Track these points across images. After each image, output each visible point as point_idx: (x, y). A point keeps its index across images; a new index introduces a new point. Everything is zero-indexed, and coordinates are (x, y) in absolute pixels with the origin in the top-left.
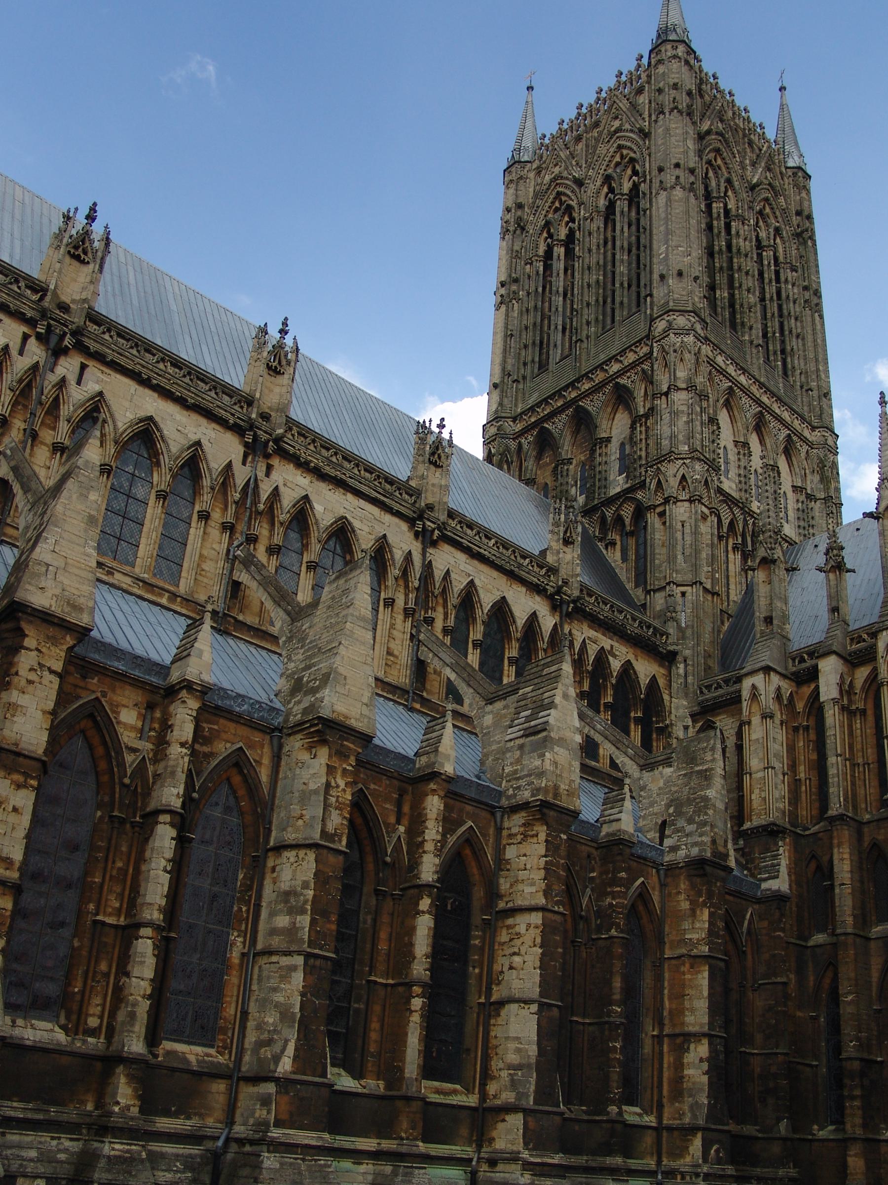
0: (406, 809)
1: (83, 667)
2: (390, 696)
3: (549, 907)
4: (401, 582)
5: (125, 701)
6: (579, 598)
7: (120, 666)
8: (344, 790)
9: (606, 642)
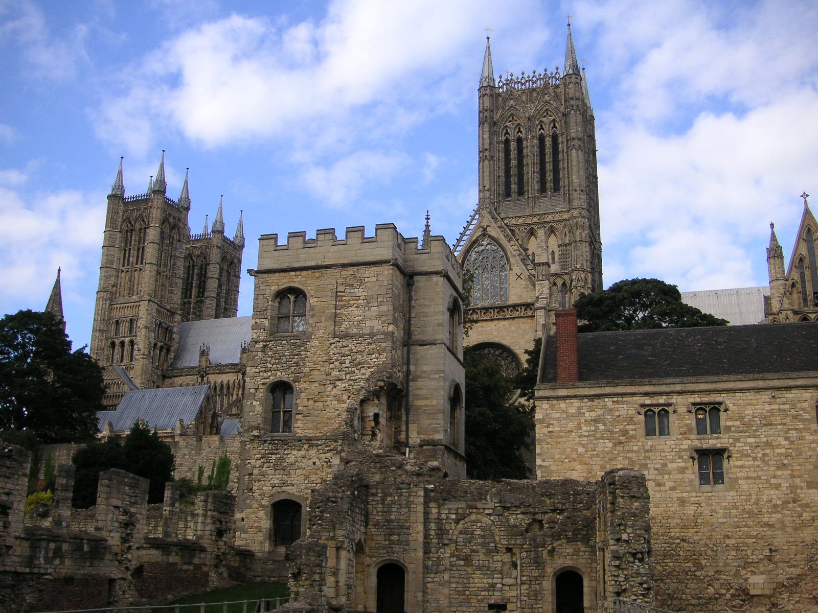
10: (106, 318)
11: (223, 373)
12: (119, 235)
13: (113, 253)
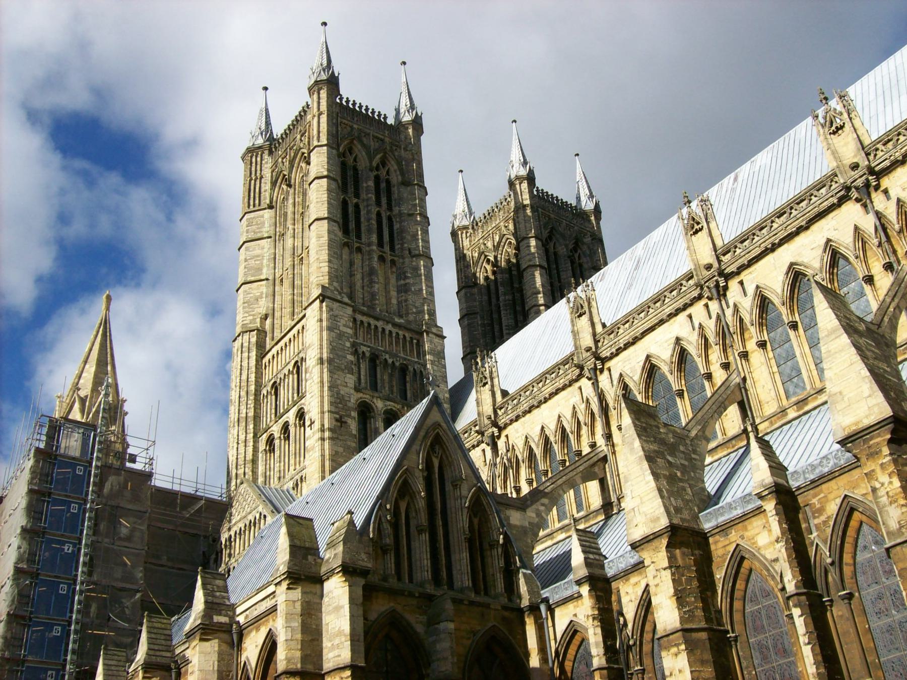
1: (723, 530)
5: (757, 531)
7: (739, 512)
8: (891, 483)
10: (252, 388)
11: (538, 407)
12: (268, 214)
13: (258, 252)
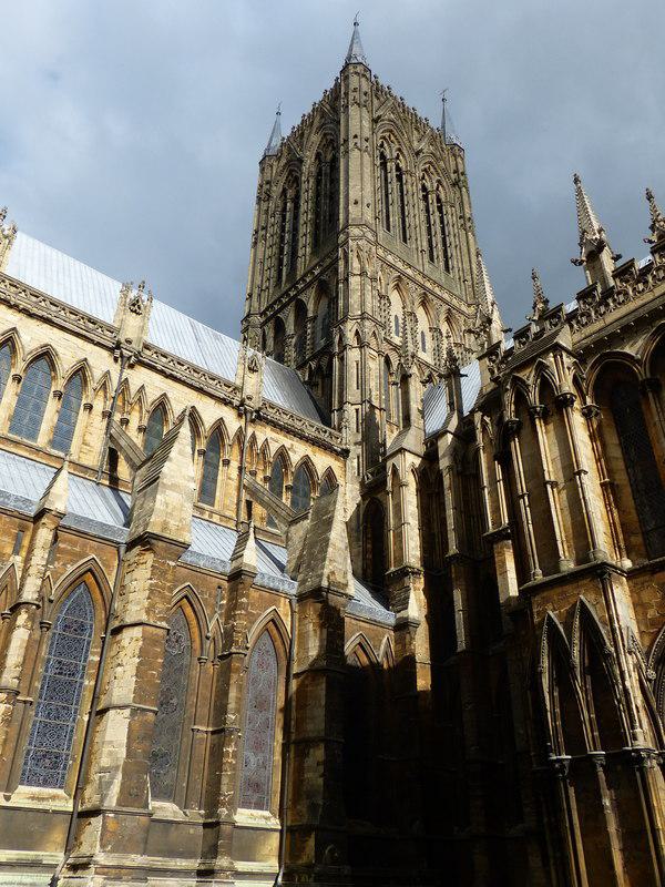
0: (26, 542)
2: (81, 475)
3: (152, 622)
4: (101, 393)
6: (260, 409)
9: (287, 441)
